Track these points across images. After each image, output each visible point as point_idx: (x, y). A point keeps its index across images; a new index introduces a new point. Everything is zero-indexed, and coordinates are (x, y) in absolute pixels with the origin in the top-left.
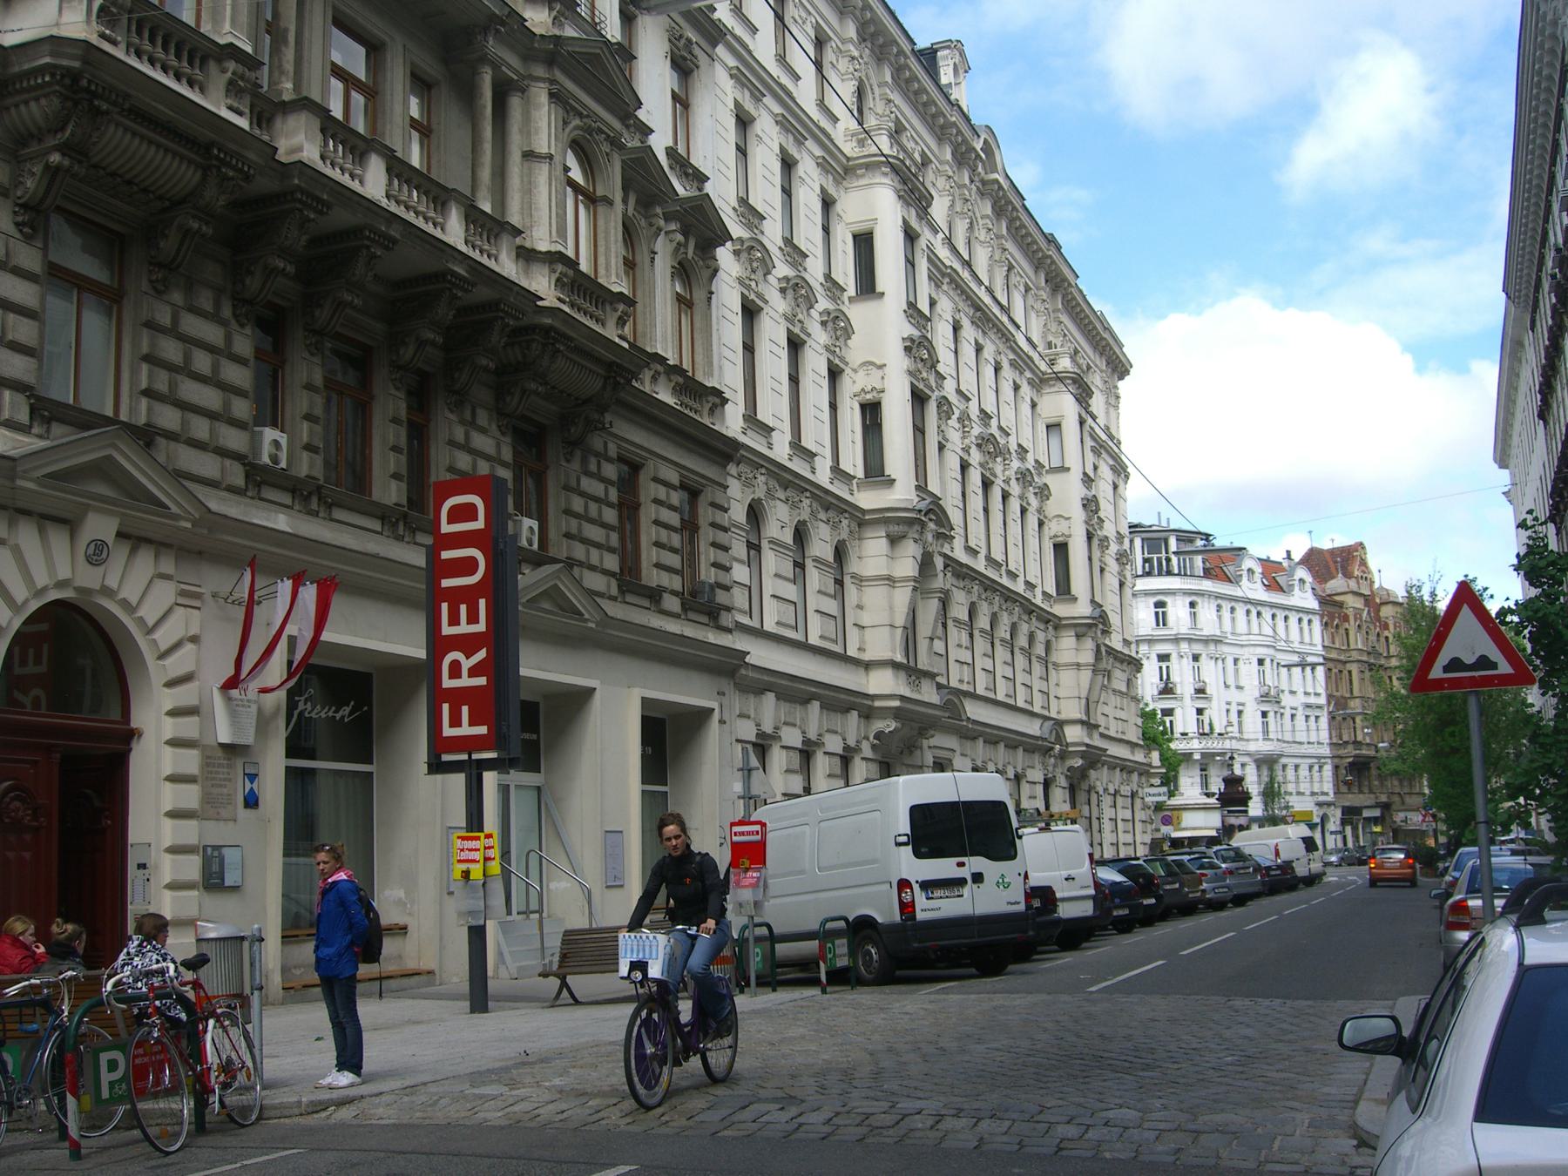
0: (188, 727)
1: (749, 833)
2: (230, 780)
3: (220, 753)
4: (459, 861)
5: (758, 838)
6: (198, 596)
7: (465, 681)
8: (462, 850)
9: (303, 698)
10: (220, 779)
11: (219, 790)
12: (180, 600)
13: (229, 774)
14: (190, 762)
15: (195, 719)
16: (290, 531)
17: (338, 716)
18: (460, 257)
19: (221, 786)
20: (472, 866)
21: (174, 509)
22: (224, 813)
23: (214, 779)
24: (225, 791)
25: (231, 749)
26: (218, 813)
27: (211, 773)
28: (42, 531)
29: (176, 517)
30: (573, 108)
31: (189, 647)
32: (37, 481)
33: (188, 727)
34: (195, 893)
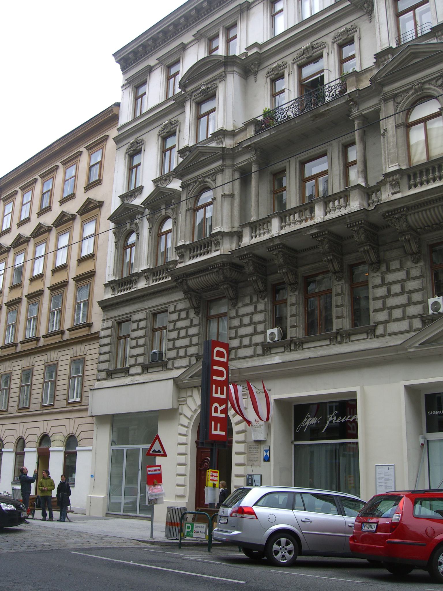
1: (155, 470)
2: (258, 452)
3: (254, 444)
4: (211, 480)
5: (160, 472)
7: (219, 415)
8: (212, 476)
9: (332, 416)
13: (257, 450)
16: (281, 361)
17: (351, 420)
18: (309, 228)
19: (254, 455)
20: (215, 482)
22: (255, 464)
24: (256, 456)
25: (259, 442)
30: (403, 92)
32: (187, 380)
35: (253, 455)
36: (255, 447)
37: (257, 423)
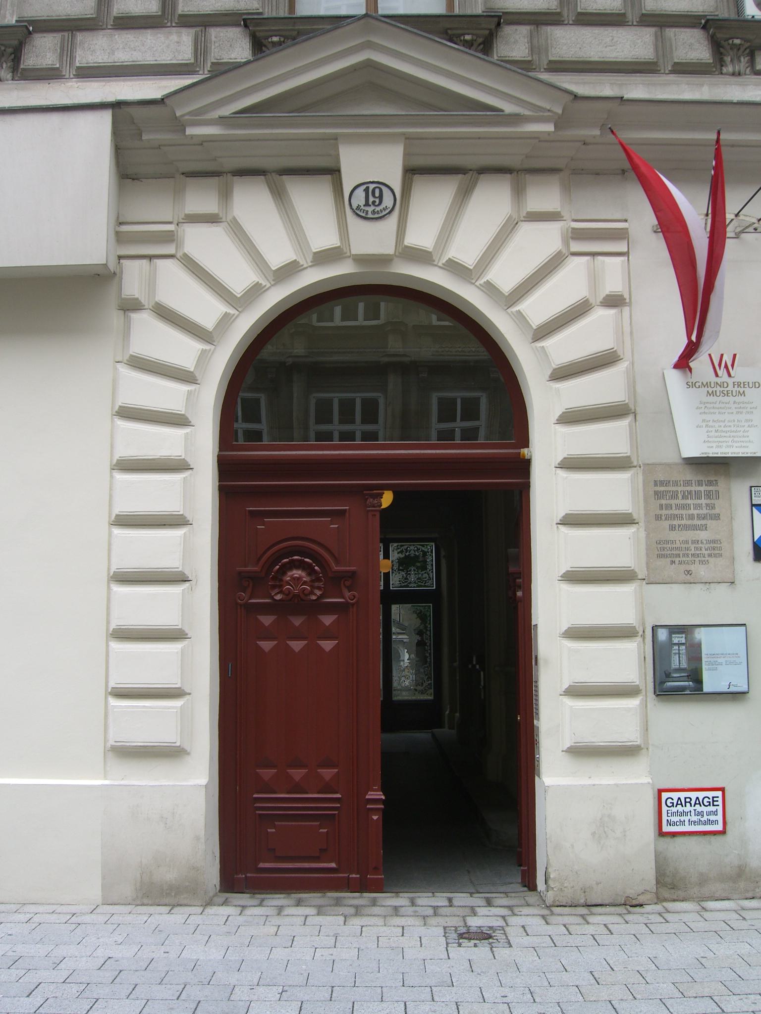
2: (717, 517)
6: (620, 235)
10: (691, 517)
11: (691, 535)
12: (575, 247)
15: (623, 424)
19: (695, 528)
21: (509, 108)
22: (701, 571)
23: (675, 517)
24: (703, 535)
26: (689, 572)
28: (279, 195)
29: (516, 119)
31: (601, 315)
32: (223, 121)
34: (633, 703)
35: (687, 528)
36: (694, 488)
37: (722, 372)
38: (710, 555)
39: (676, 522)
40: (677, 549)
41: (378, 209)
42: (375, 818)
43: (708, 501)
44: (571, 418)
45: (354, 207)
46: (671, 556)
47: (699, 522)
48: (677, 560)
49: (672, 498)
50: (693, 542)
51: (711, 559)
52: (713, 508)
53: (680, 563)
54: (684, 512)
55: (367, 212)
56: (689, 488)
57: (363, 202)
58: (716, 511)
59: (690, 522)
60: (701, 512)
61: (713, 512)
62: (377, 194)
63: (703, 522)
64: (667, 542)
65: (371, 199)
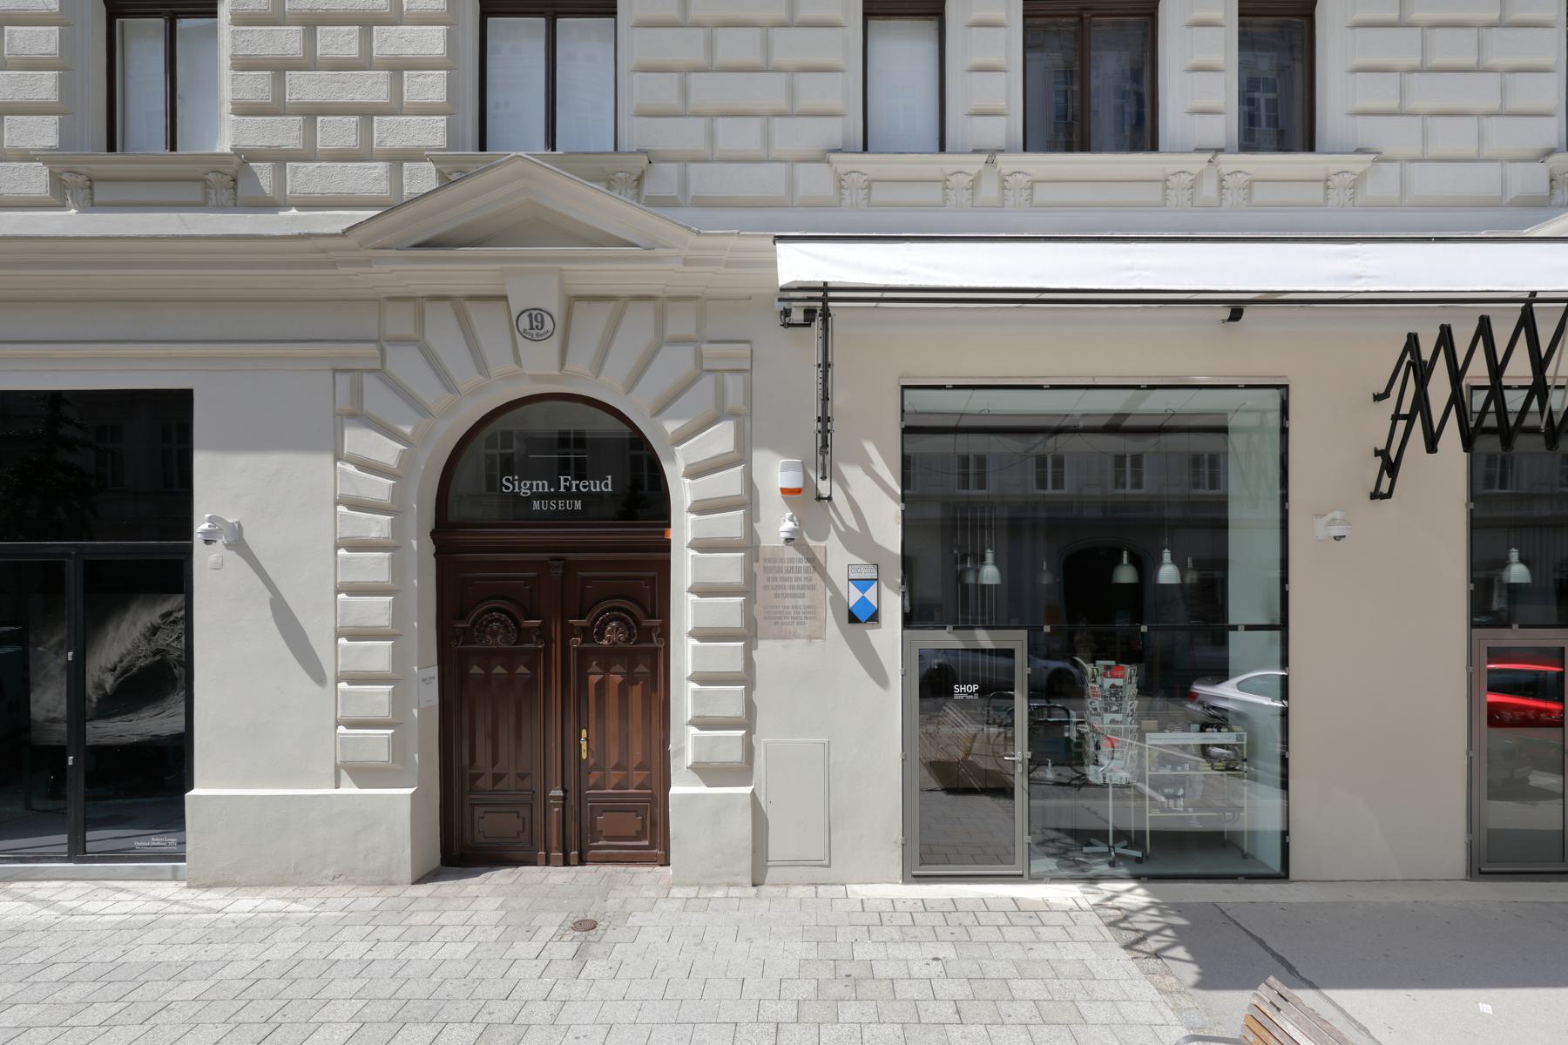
0: (730, 524)
2: (813, 588)
10: (792, 588)
14: (729, 567)
19: (794, 596)
23: (779, 587)
24: (800, 602)
27: (775, 579)
33: (730, 524)
38: (806, 618)
39: (780, 592)
40: (780, 612)
41: (541, 332)
42: (556, 810)
43: (807, 575)
44: (701, 508)
45: (521, 330)
46: (775, 618)
47: (799, 592)
48: (779, 621)
49: (778, 572)
50: (793, 607)
51: (808, 621)
52: (810, 580)
53: (782, 624)
54: (787, 583)
55: (532, 336)
56: (791, 565)
57: (528, 327)
58: (813, 582)
59: (791, 592)
60: (800, 583)
61: (811, 583)
62: (539, 319)
63: (802, 592)
64: (772, 607)
65: (535, 324)
